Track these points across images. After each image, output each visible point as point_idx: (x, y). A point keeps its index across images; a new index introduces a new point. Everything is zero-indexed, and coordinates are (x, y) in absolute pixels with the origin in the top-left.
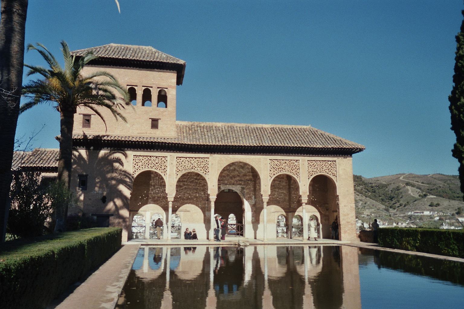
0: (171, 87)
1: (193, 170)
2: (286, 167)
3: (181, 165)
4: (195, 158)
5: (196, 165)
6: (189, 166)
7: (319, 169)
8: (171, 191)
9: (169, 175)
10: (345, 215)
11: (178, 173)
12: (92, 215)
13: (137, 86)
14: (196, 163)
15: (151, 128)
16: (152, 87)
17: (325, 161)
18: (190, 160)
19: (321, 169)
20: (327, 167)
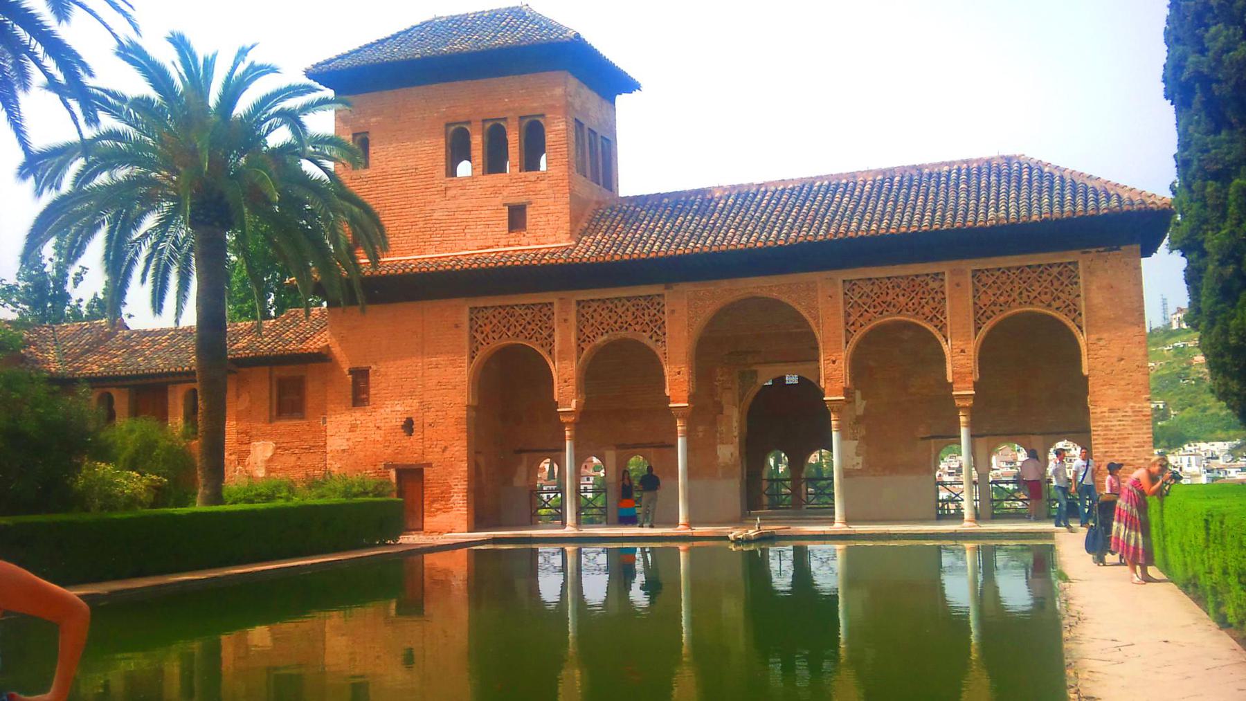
0: (553, 107)
1: (623, 334)
2: (901, 298)
3: (591, 321)
4: (628, 299)
5: (629, 319)
6: (611, 322)
7: (1015, 295)
8: (567, 396)
9: (560, 352)
10: (1110, 441)
11: (583, 345)
12: (387, 467)
13: (469, 122)
14: (629, 313)
15: (510, 231)
16: (505, 119)
17: (1039, 266)
18: (610, 306)
19: (1025, 293)
20: (1045, 284)
